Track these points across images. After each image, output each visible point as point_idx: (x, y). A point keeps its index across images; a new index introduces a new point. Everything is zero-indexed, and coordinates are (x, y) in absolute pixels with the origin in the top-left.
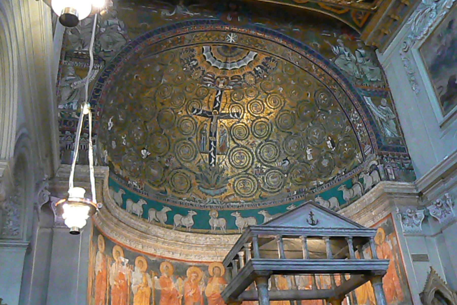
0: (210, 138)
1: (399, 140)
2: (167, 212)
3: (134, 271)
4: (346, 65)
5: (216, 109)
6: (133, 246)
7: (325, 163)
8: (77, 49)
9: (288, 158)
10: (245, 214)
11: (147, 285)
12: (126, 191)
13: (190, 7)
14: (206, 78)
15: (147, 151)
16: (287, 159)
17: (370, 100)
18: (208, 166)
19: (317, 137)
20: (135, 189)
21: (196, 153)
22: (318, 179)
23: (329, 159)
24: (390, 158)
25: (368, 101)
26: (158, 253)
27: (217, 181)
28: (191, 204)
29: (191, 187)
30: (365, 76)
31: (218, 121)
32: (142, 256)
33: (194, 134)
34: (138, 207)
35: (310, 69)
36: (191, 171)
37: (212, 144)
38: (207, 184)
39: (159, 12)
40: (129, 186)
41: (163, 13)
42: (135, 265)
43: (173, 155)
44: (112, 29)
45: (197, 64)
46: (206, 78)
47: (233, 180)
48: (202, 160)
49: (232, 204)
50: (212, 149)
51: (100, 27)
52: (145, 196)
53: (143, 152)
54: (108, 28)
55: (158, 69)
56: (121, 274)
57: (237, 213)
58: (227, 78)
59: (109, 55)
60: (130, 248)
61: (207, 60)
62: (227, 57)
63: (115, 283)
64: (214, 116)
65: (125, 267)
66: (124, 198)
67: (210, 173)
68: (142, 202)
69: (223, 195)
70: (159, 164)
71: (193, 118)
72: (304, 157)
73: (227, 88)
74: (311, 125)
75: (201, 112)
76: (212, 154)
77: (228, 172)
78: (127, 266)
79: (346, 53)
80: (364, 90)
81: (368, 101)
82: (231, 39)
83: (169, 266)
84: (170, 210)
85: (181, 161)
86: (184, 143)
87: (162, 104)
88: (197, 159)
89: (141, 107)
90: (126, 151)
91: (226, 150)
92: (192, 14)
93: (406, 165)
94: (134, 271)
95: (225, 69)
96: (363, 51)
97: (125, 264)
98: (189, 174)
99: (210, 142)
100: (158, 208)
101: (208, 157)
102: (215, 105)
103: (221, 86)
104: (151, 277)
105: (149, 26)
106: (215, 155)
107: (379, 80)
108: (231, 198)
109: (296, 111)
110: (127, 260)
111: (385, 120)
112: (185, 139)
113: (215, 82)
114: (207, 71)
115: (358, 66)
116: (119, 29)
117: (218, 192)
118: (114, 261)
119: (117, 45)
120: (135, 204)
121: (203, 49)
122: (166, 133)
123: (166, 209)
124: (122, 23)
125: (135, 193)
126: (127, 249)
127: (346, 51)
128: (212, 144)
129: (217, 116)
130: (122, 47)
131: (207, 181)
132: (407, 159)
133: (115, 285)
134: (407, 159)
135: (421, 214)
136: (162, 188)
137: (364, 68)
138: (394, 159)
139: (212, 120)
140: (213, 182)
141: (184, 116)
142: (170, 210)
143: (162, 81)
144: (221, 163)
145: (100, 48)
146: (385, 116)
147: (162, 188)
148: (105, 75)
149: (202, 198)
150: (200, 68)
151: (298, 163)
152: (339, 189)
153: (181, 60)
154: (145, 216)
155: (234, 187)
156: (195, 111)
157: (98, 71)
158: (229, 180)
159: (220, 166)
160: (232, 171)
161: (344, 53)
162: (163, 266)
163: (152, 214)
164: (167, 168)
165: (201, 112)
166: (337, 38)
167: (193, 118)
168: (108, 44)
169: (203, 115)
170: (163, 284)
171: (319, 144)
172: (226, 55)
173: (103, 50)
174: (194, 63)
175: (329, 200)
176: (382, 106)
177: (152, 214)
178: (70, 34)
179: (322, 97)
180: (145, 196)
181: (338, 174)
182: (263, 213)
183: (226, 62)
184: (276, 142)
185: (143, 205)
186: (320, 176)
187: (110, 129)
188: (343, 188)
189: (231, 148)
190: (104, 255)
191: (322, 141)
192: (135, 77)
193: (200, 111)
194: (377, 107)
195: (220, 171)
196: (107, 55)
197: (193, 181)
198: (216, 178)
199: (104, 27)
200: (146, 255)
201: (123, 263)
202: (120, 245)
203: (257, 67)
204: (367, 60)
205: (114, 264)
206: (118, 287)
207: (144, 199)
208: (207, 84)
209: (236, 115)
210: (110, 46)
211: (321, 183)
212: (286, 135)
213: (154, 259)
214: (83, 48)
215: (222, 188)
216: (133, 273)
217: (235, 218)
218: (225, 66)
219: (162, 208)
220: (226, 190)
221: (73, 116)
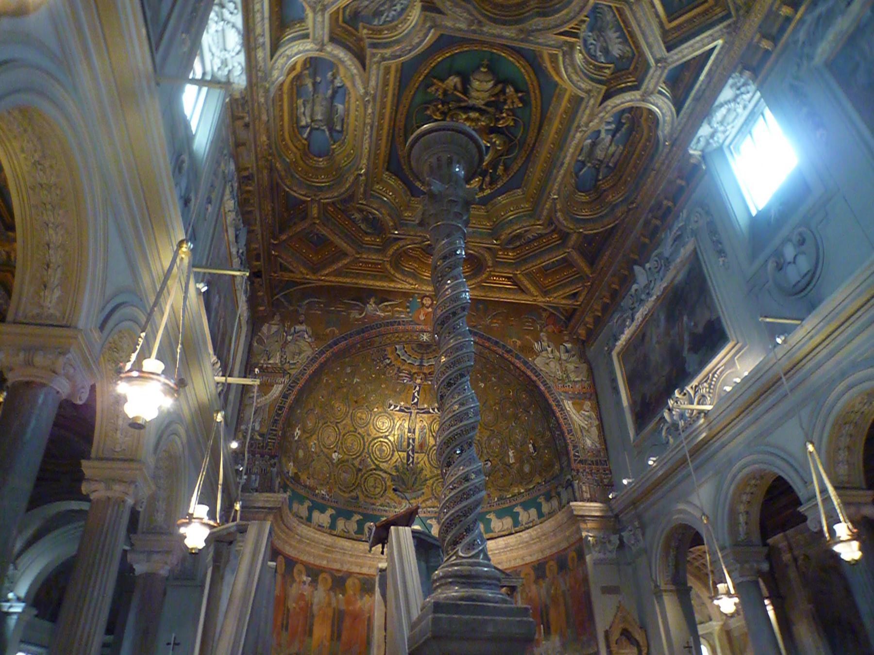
0: (409, 434)
1: (599, 451)
2: (358, 521)
3: (316, 589)
4: (547, 364)
5: (415, 403)
6: (318, 562)
7: (527, 468)
8: (262, 362)
9: (491, 459)
11: (329, 604)
12: (312, 502)
13: (380, 306)
14: (401, 374)
15: (339, 453)
16: (488, 460)
17: (571, 405)
18: (406, 466)
19: (519, 438)
20: (323, 498)
21: (393, 451)
22: (519, 485)
23: (531, 464)
24: (588, 472)
25: (568, 405)
26: (345, 568)
27: (414, 483)
28: (385, 510)
29: (386, 490)
30: (568, 376)
31: (418, 416)
32: (325, 572)
33: (392, 430)
34: (324, 518)
35: (509, 367)
36: (386, 472)
37: (411, 441)
38: (404, 487)
39: (349, 314)
40: (316, 495)
41: (352, 316)
42: (318, 583)
43: (367, 456)
44: (299, 336)
45: (391, 362)
46: (401, 374)
47: (431, 481)
48: (399, 460)
49: (429, 509)
50: (411, 447)
51: (287, 336)
52: (335, 505)
54: (295, 335)
55: (349, 370)
56: (302, 595)
57: (434, 520)
58: (424, 374)
59: (293, 367)
60: (315, 565)
61: (403, 358)
62: (422, 354)
63: (294, 605)
64: (413, 411)
65: (306, 587)
66: (310, 510)
67: (407, 473)
68: (330, 512)
69: (420, 499)
70: (351, 466)
71: (389, 414)
72: (507, 459)
73: (425, 383)
74: (514, 424)
75: (398, 408)
76: (410, 453)
78: (309, 585)
79: (549, 349)
80: (565, 392)
81: (568, 405)
82: (425, 337)
83: (356, 581)
84: (361, 517)
85: (376, 462)
86: (380, 441)
87: (356, 402)
88: (394, 459)
89: (332, 408)
90: (315, 457)
91: (426, 448)
92: (383, 314)
93: (605, 480)
94: (316, 589)
95: (421, 365)
96: (569, 346)
97: (307, 583)
98: (384, 475)
99: (409, 438)
100: (348, 516)
101: (406, 455)
102: (413, 400)
103: (418, 381)
104: (336, 595)
105: (337, 331)
106: (413, 454)
107: (584, 379)
108: (429, 503)
109: (499, 408)
110: (310, 579)
111: (586, 427)
112: (382, 437)
113: (412, 376)
114: (404, 367)
115: (561, 364)
116: (306, 336)
117: (414, 495)
118: (294, 581)
119: (302, 356)
120: (322, 515)
121: (396, 348)
122: (361, 432)
123: (357, 517)
124: (309, 330)
125: (325, 502)
126: (311, 566)
127: (549, 347)
128: (411, 441)
129: (416, 411)
130: (308, 357)
131: (404, 483)
132: (607, 474)
133: (294, 608)
134: (607, 474)
136: (354, 494)
138: (591, 474)
139: (411, 416)
140: (411, 483)
141: (381, 413)
142: (361, 517)
143: (355, 381)
144: (418, 463)
145: (286, 359)
146: (586, 423)
147: (354, 494)
148: (290, 390)
149: (397, 502)
150: (394, 365)
151: (501, 465)
152: (539, 500)
153: (374, 360)
154: (333, 526)
155: (432, 490)
156: (392, 407)
157: (282, 385)
158: (428, 482)
159: (419, 465)
160: (431, 472)
161: (547, 350)
162: (350, 582)
163: (341, 524)
164: (360, 470)
165: (398, 408)
166: (541, 331)
167: (389, 414)
168: (294, 354)
169: (401, 410)
170: (348, 602)
171: (521, 446)
172: (422, 352)
173: (289, 362)
174: (388, 361)
175: (530, 511)
176: (584, 410)
177: (341, 524)
178: (255, 344)
179: (524, 396)
180: (335, 505)
181: (538, 483)
183: (422, 359)
184: (479, 441)
185: (331, 516)
186: (521, 483)
187: (296, 438)
188: (541, 500)
189: (431, 445)
190: (284, 576)
191: (524, 443)
192: (325, 381)
193: (397, 406)
194: (578, 412)
195: (418, 471)
196: (293, 367)
197: (389, 483)
198: (413, 479)
199: (290, 335)
200: (330, 571)
201: (304, 583)
202: (303, 563)
204: (573, 356)
205: (294, 585)
206: (298, 609)
207: (332, 508)
208: (404, 380)
209: (436, 410)
210: (296, 357)
211: (522, 491)
212: (489, 433)
213: (340, 575)
214: (268, 360)
215: (419, 490)
216: (316, 592)
218: (421, 362)
219: (352, 516)
220: (423, 493)
221: (255, 437)
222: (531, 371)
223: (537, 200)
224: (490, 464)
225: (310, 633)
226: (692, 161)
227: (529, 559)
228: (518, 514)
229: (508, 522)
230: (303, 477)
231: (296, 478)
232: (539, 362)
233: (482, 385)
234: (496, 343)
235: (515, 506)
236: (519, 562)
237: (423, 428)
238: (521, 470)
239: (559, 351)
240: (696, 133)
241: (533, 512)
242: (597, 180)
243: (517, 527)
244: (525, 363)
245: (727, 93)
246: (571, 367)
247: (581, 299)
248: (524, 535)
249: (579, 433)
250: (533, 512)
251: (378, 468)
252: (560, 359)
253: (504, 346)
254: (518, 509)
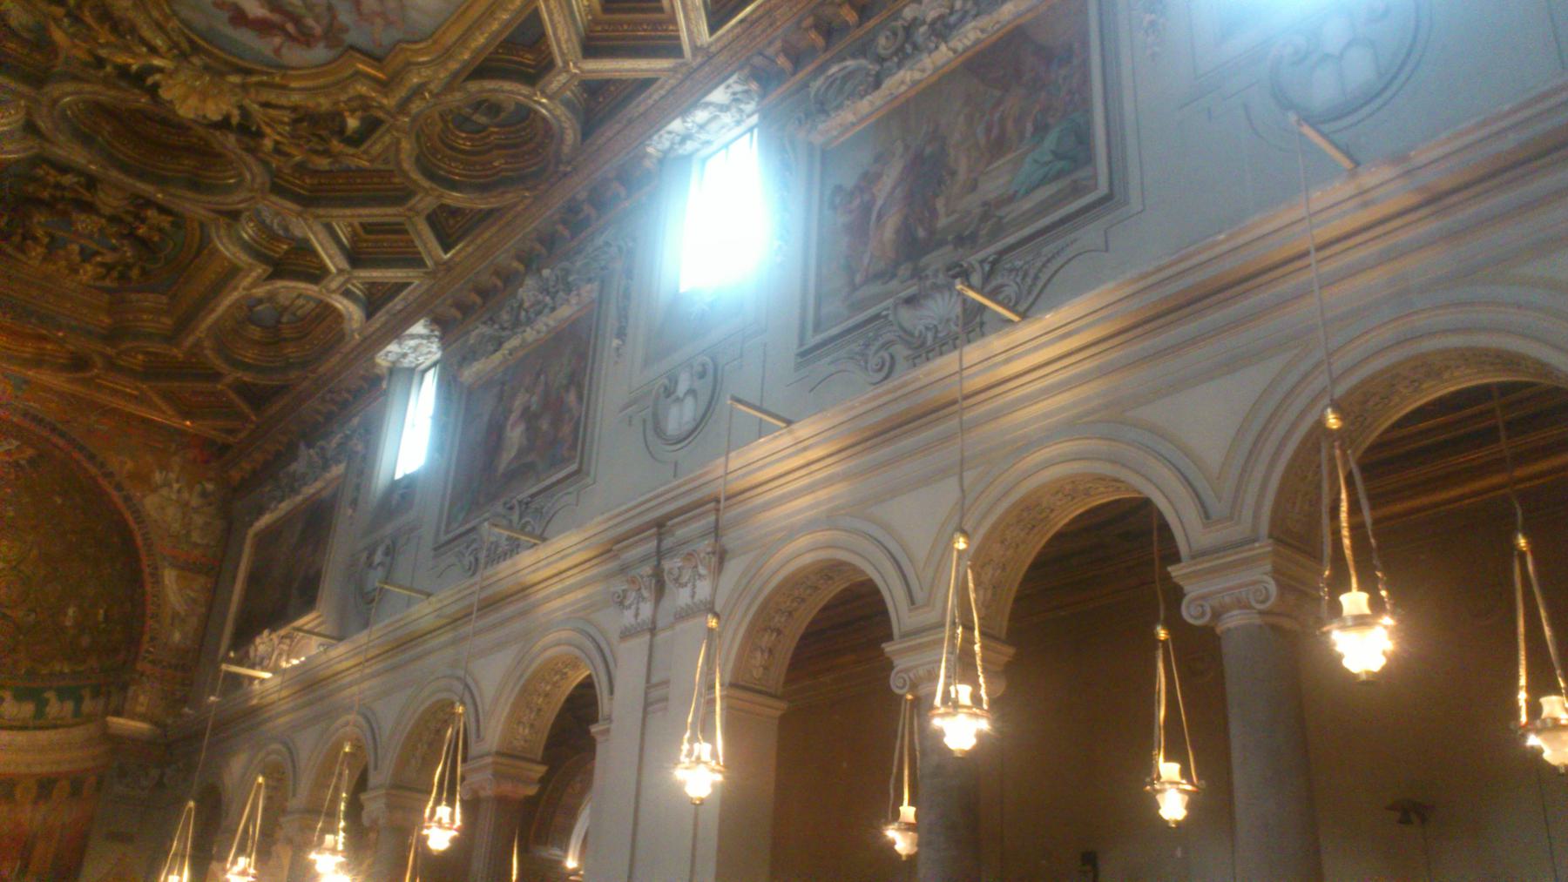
7: (86, 641)
9: (38, 610)
16: (34, 610)
25: (169, 576)
81: (169, 576)
96: (210, 487)
107: (212, 543)
127: (177, 481)
135: (154, 773)
137: (195, 517)
161: (170, 486)
188: (87, 693)
203: (23, 459)
204: (210, 504)
211: (66, 670)
222: (133, 512)
223: (185, 323)
224: (33, 616)
226: (378, 371)
227: (37, 769)
228: (46, 702)
229: (28, 709)
232: (150, 503)
233: (59, 501)
234: (92, 458)
235: (50, 688)
236: (23, 769)
239: (191, 489)
240: (385, 347)
241: (69, 706)
242: (279, 322)
243: (39, 722)
244: (127, 499)
245: (419, 328)
246: (199, 520)
247: (242, 435)
248: (42, 737)
249: (168, 620)
252: (187, 504)
253: (102, 465)
254: (51, 695)
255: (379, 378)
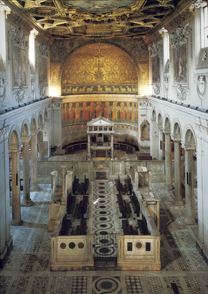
7: (130, 77)
10: (108, 87)
34: (75, 90)
53: (77, 72)
66: (72, 89)
77: (104, 73)
100: (82, 87)
123: (85, 87)
135: (146, 103)
162: (83, 104)
163: (80, 90)
170: (84, 109)
177: (80, 90)
182: (113, 87)
188: (132, 87)
197: (93, 76)
200: (79, 102)
217: (105, 88)
225: (75, 117)
230: (69, 82)
231: (67, 83)
237: (102, 61)
238: (128, 77)
246: (142, 53)
250: (131, 89)
251: (90, 73)
254: (127, 87)
255: (161, 35)
